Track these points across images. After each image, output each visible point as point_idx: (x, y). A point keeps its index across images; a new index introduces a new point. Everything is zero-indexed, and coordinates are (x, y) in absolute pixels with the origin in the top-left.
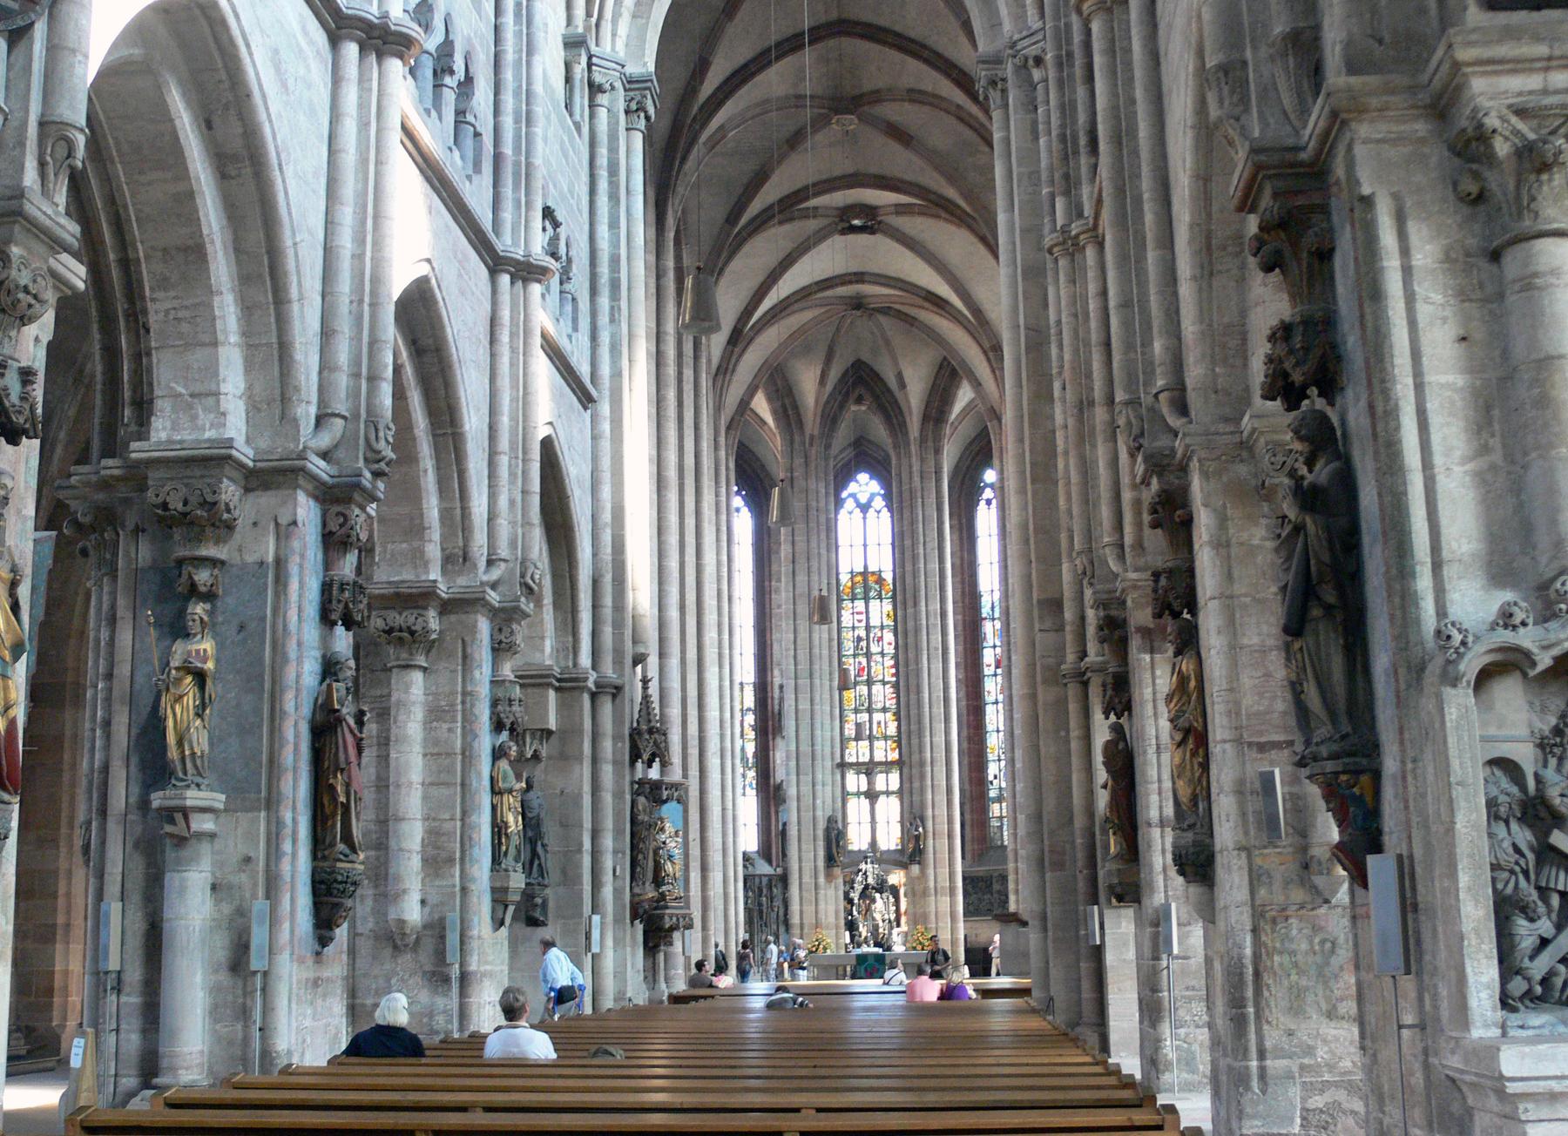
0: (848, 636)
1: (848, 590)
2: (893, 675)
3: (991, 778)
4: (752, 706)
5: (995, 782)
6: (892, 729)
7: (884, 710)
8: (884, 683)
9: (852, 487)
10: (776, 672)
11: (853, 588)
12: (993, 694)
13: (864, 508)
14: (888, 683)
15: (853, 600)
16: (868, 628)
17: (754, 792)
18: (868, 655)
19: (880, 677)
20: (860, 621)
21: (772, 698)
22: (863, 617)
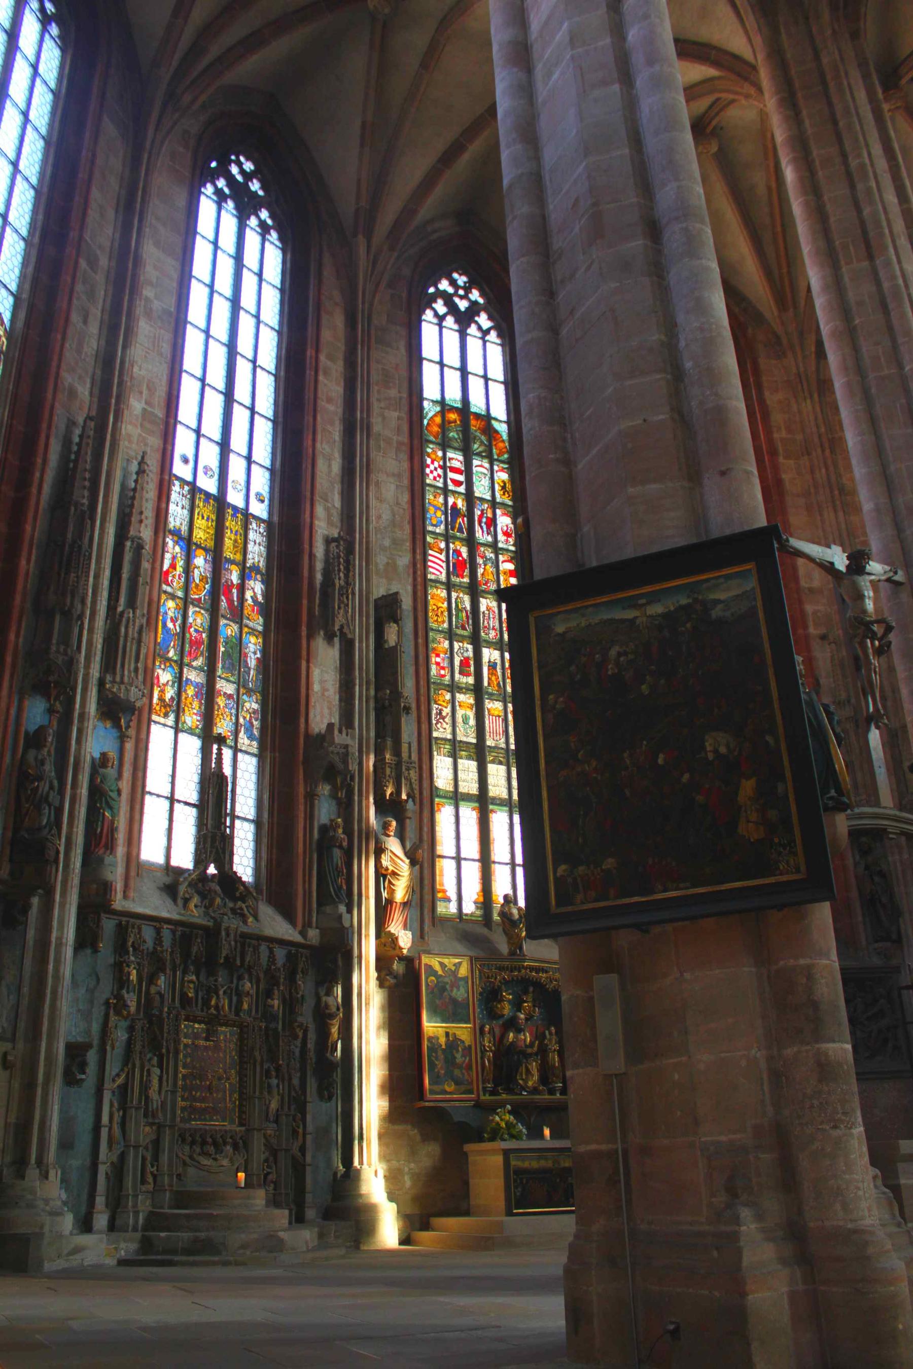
0: (434, 500)
1: (436, 429)
9: (444, 285)
10: (320, 510)
11: (444, 426)
13: (465, 319)
17: (254, 747)
18: (471, 542)
20: (457, 483)
21: (312, 556)
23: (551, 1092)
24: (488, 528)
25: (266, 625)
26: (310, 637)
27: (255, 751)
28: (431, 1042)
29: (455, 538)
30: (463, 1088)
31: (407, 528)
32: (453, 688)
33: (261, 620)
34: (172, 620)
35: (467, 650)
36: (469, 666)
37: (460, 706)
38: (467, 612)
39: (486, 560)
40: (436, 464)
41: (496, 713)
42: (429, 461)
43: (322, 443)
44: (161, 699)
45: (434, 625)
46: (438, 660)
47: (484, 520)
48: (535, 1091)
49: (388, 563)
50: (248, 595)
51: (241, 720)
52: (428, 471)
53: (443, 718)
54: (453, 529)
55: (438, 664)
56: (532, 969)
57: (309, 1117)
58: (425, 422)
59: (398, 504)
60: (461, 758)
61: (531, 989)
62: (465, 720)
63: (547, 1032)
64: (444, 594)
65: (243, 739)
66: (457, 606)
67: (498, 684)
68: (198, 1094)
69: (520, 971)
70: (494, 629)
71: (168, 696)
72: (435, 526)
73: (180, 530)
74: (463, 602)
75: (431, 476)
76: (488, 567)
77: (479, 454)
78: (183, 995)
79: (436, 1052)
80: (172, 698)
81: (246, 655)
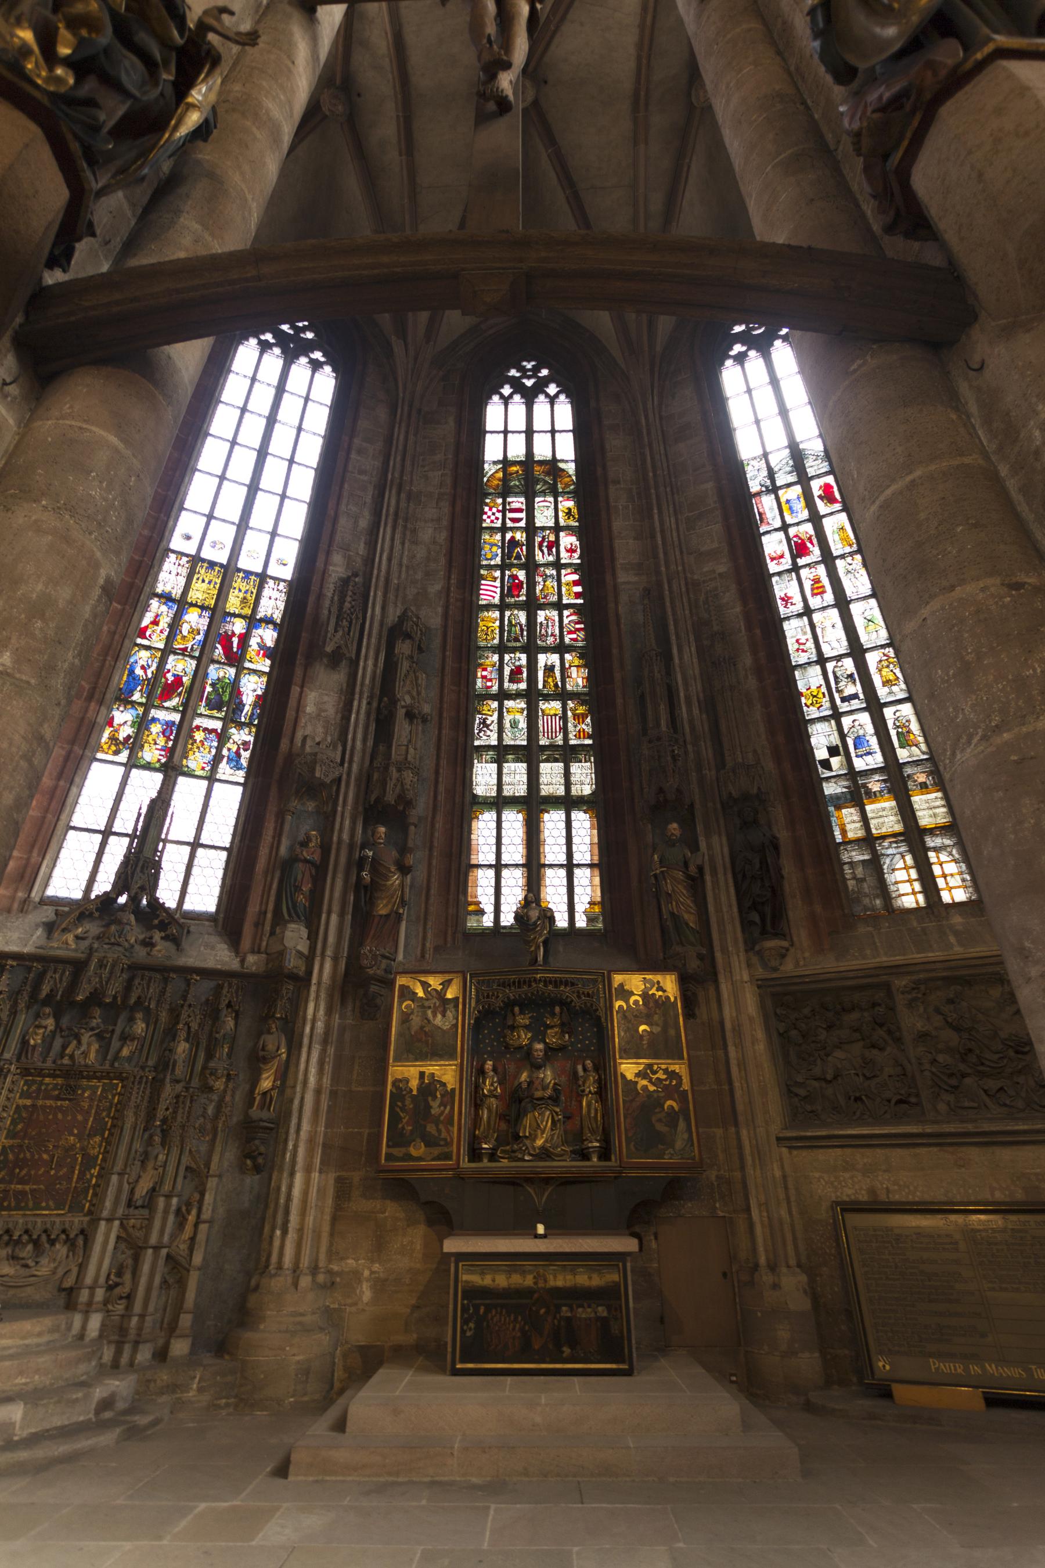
2: (578, 595)
3: (821, 754)
4: (278, 616)
5: (835, 762)
6: (577, 679)
7: (561, 649)
8: (559, 606)
10: (337, 558)
12: (797, 598)
14: (568, 606)
15: (504, 495)
16: (531, 529)
17: (240, 776)
18: (531, 567)
19: (555, 598)
22: (523, 515)
23: (584, 1156)
24: (549, 548)
25: (272, 667)
26: (308, 665)
27: (242, 780)
28: (398, 1088)
29: (512, 566)
30: (436, 1151)
31: (443, 561)
32: (503, 696)
33: (268, 662)
34: (143, 667)
35: (520, 659)
36: (521, 673)
37: (508, 712)
38: (521, 626)
39: (546, 578)
40: (494, 510)
41: (552, 712)
42: (486, 509)
43: (347, 505)
44: (113, 739)
45: (482, 644)
46: (485, 673)
47: (545, 544)
48: (545, 1154)
49: (418, 593)
50: (254, 642)
51: (225, 752)
52: (485, 517)
53: (487, 726)
54: (509, 558)
55: (484, 677)
56: (547, 982)
57: (208, 1198)
58: (485, 479)
59: (434, 542)
60: (507, 762)
61: (557, 1009)
62: (514, 724)
63: (580, 1068)
64: (497, 614)
65: (225, 770)
66: (510, 621)
67: (556, 685)
68: (24, 1172)
69: (530, 986)
70: (552, 635)
71: (122, 736)
72: (491, 559)
73: (170, 593)
74: (517, 617)
75: (488, 521)
76: (548, 583)
77: (544, 493)
78: (24, 1042)
79: (402, 1098)
80: (129, 737)
81: (239, 693)
